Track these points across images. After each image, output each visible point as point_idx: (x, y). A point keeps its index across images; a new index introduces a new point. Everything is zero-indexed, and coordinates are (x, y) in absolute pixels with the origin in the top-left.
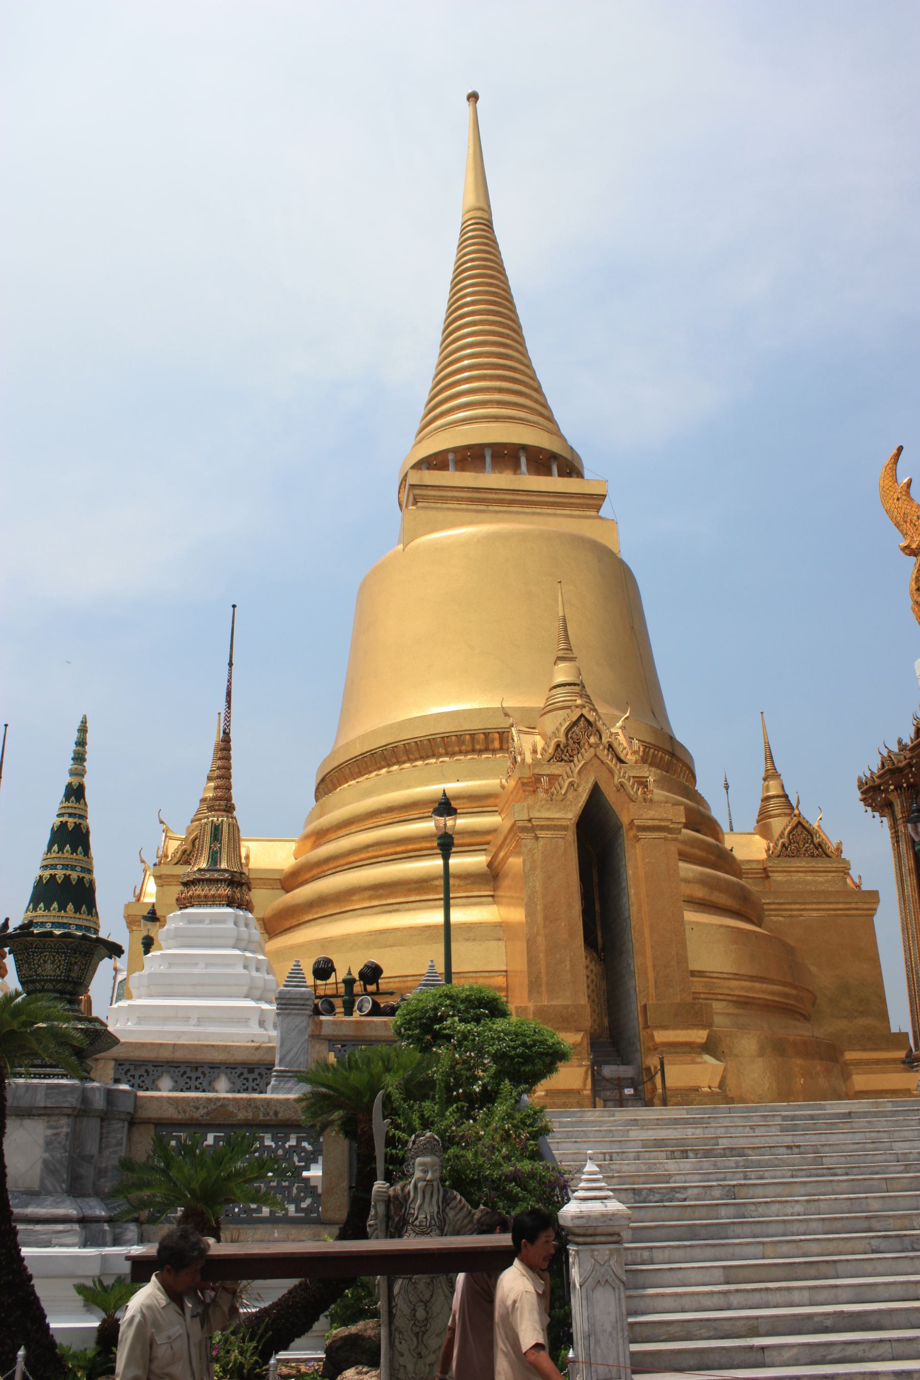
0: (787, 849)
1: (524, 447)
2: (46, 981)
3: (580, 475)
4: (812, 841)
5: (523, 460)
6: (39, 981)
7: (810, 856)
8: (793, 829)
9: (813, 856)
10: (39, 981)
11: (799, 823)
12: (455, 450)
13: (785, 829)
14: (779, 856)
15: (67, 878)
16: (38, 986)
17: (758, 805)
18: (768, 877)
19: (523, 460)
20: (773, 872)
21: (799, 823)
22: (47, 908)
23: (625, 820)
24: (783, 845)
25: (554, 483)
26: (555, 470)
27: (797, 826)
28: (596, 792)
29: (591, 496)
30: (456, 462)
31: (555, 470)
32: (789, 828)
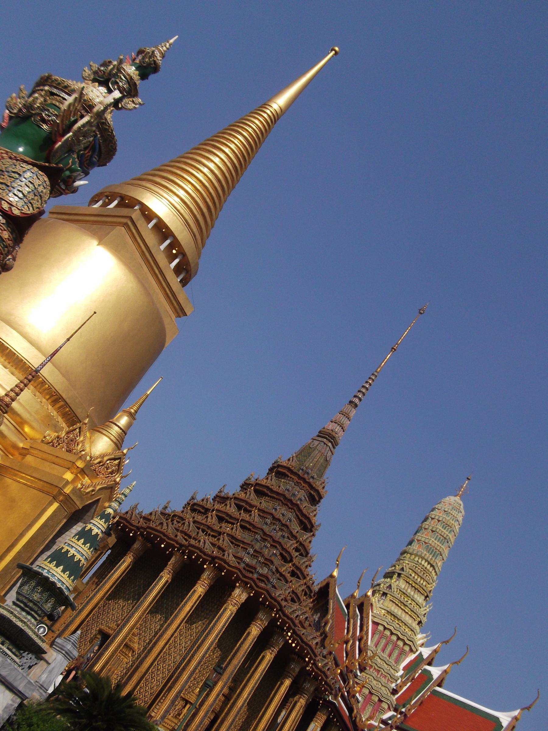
1: (184, 255)
2: (41, 609)
3: (183, 286)
5: (177, 261)
6: (39, 607)
10: (39, 607)
12: (160, 221)
15: (74, 556)
16: (36, 609)
19: (177, 261)
22: (69, 577)
25: (174, 281)
26: (181, 277)
29: (182, 309)
30: (155, 226)
31: (181, 277)
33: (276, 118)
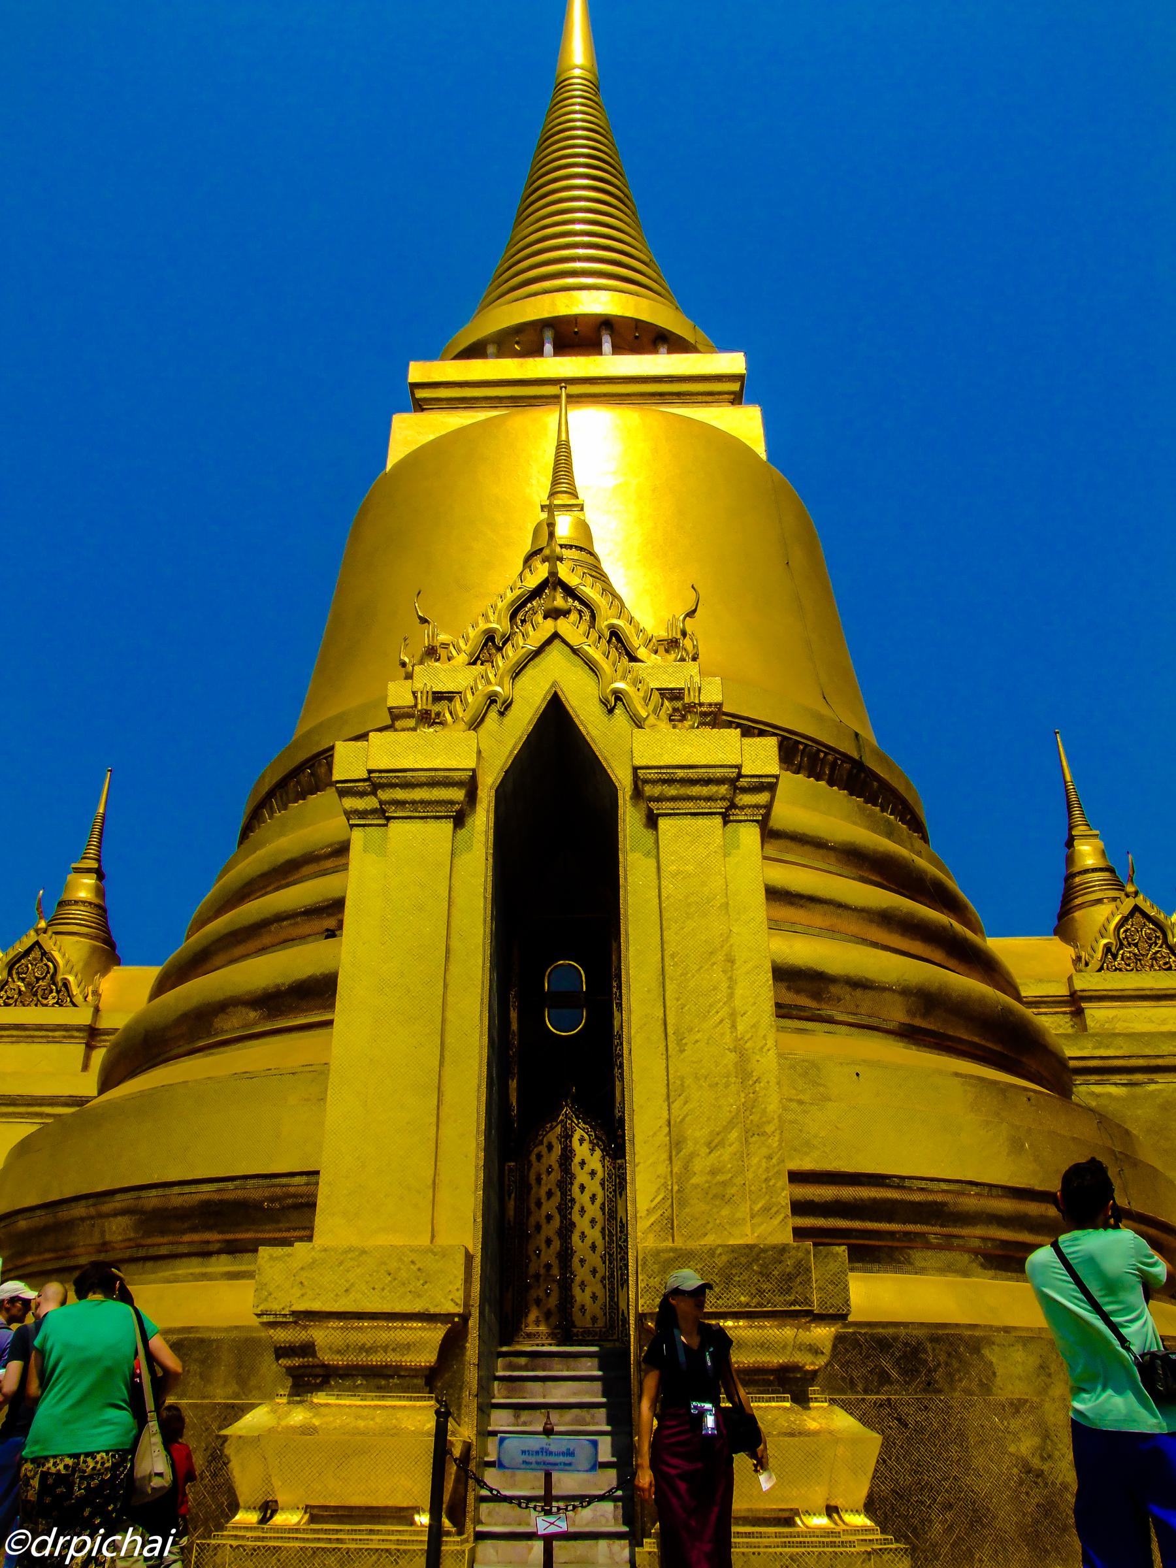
0: (1115, 957)
4: (1165, 941)
7: (1161, 968)
8: (1124, 920)
9: (1170, 969)
11: (1136, 908)
13: (1108, 920)
14: (1099, 970)
17: (1060, 887)
18: (1079, 1013)
20: (1090, 999)
21: (1136, 908)
23: (622, 777)
24: (1108, 949)
27: (1132, 914)
28: (555, 714)
32: (1118, 918)
33: (600, 85)
